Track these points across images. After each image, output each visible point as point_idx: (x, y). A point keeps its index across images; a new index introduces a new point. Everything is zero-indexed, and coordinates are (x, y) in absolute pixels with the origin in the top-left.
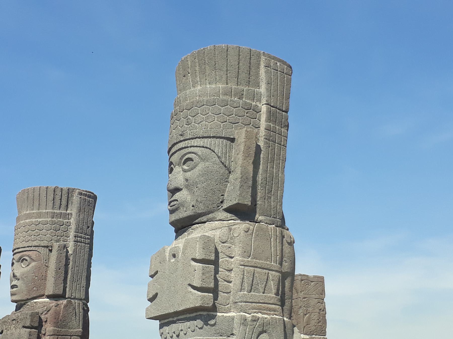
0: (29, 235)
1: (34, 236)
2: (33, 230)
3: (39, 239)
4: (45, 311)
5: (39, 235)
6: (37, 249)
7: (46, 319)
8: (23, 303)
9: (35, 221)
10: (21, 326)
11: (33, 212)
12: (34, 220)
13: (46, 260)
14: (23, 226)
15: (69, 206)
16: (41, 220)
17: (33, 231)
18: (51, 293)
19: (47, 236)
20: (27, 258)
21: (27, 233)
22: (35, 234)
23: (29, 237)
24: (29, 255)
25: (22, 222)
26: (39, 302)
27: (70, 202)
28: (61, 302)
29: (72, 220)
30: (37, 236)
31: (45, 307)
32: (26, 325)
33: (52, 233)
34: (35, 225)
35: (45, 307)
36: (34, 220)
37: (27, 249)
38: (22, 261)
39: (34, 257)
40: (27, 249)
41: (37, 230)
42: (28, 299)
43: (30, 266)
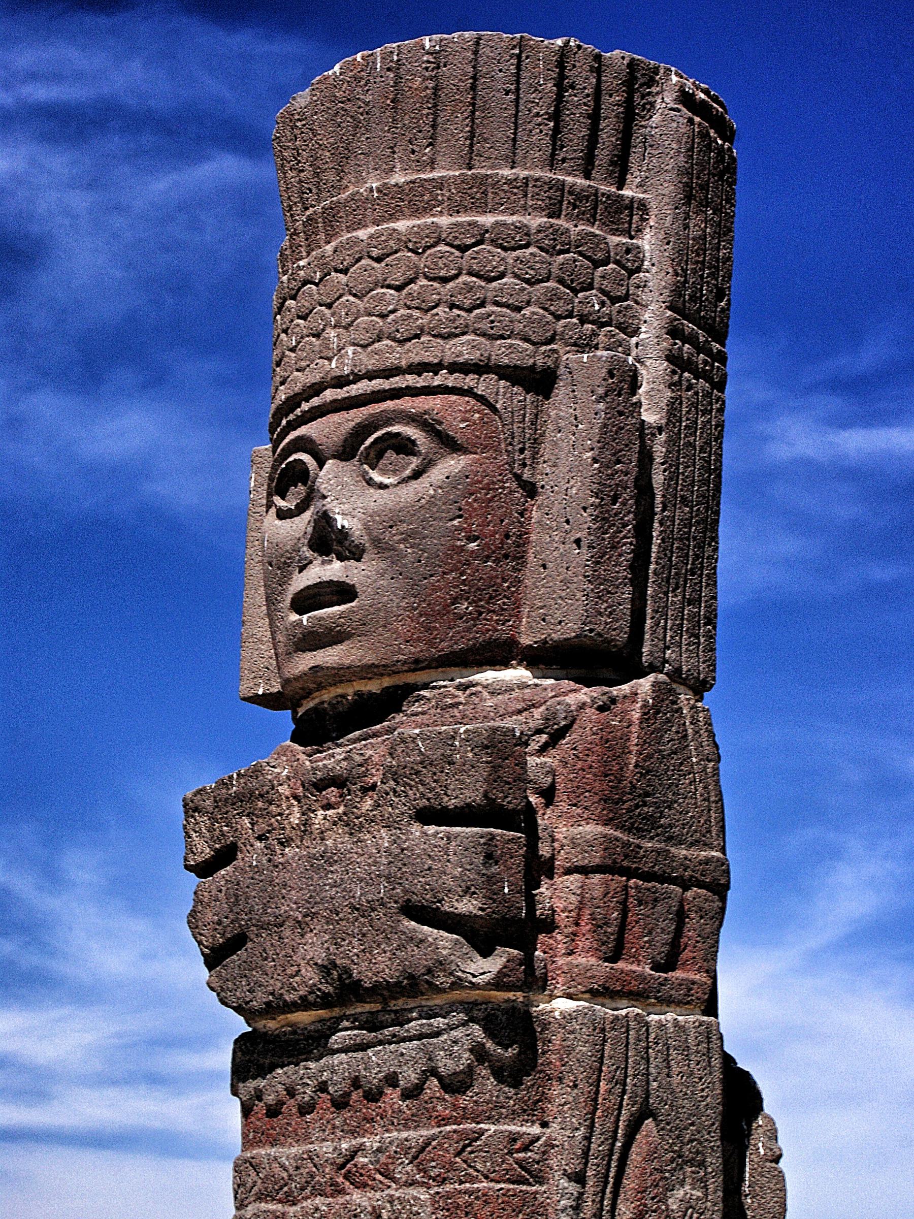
0: (415, 303)
1: (452, 306)
2: (442, 273)
3: (484, 325)
4: (539, 732)
5: (482, 305)
6: (470, 381)
7: (550, 780)
8: (374, 687)
9: (456, 224)
10: (400, 807)
11: (435, 174)
12: (444, 221)
13: (522, 451)
14: (375, 252)
15: (633, 159)
16: (487, 220)
17: (445, 280)
18: (568, 630)
19: (526, 312)
20: (410, 431)
21: (405, 292)
22: (458, 299)
23: (416, 313)
24: (426, 413)
25: (362, 234)
26: (485, 687)
27: (637, 139)
28: (626, 688)
29: (647, 242)
30: (469, 311)
31: (537, 713)
32: (452, 803)
33: (554, 296)
34: (458, 248)
35: (537, 713)
36: (444, 221)
37: (419, 381)
38: (374, 458)
39: (456, 426)
40: (411, 380)
41: (470, 274)
42: (417, 665)
43: (437, 474)
